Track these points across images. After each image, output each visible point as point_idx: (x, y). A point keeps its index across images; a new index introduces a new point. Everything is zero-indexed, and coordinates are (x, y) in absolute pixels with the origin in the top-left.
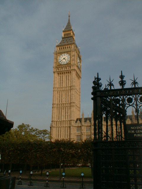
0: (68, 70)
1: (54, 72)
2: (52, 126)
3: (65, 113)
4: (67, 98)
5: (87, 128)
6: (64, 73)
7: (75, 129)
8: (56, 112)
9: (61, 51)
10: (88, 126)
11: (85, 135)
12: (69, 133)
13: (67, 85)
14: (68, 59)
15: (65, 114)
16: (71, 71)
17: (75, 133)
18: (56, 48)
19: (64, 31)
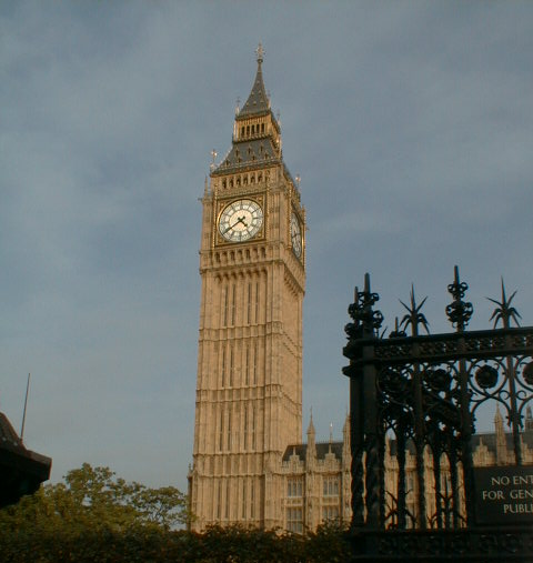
0: (255, 265)
1: (204, 272)
2: (196, 474)
3: (243, 423)
4: (252, 370)
5: (325, 483)
6: (242, 273)
7: (283, 484)
8: (209, 421)
9: (230, 191)
10: (330, 474)
11: (319, 508)
12: (258, 499)
13: (253, 318)
14: (255, 222)
15: (242, 428)
16: (267, 268)
17: (282, 500)
18: (209, 179)
19: (239, 118)
